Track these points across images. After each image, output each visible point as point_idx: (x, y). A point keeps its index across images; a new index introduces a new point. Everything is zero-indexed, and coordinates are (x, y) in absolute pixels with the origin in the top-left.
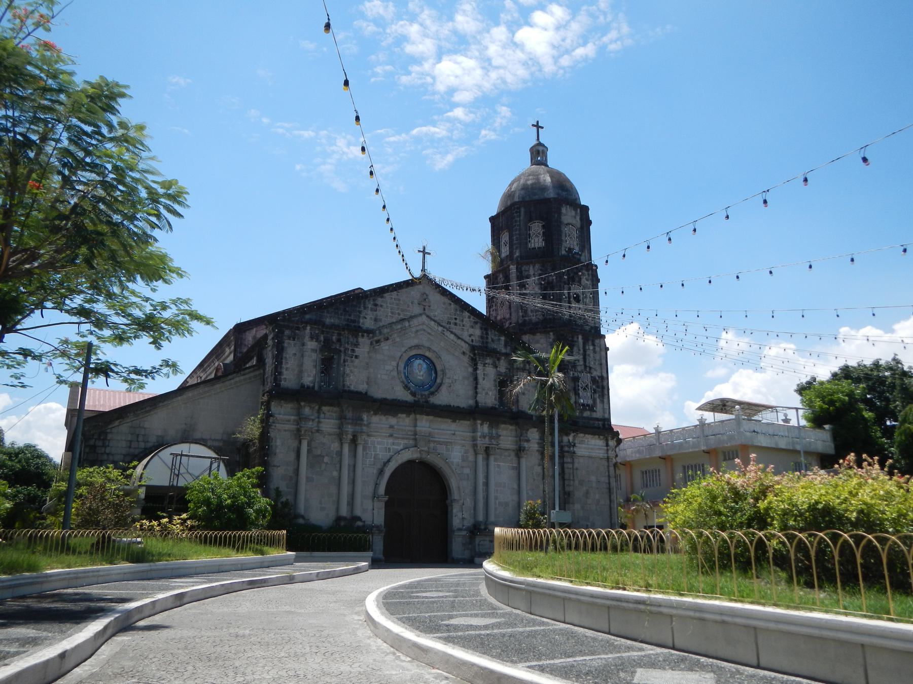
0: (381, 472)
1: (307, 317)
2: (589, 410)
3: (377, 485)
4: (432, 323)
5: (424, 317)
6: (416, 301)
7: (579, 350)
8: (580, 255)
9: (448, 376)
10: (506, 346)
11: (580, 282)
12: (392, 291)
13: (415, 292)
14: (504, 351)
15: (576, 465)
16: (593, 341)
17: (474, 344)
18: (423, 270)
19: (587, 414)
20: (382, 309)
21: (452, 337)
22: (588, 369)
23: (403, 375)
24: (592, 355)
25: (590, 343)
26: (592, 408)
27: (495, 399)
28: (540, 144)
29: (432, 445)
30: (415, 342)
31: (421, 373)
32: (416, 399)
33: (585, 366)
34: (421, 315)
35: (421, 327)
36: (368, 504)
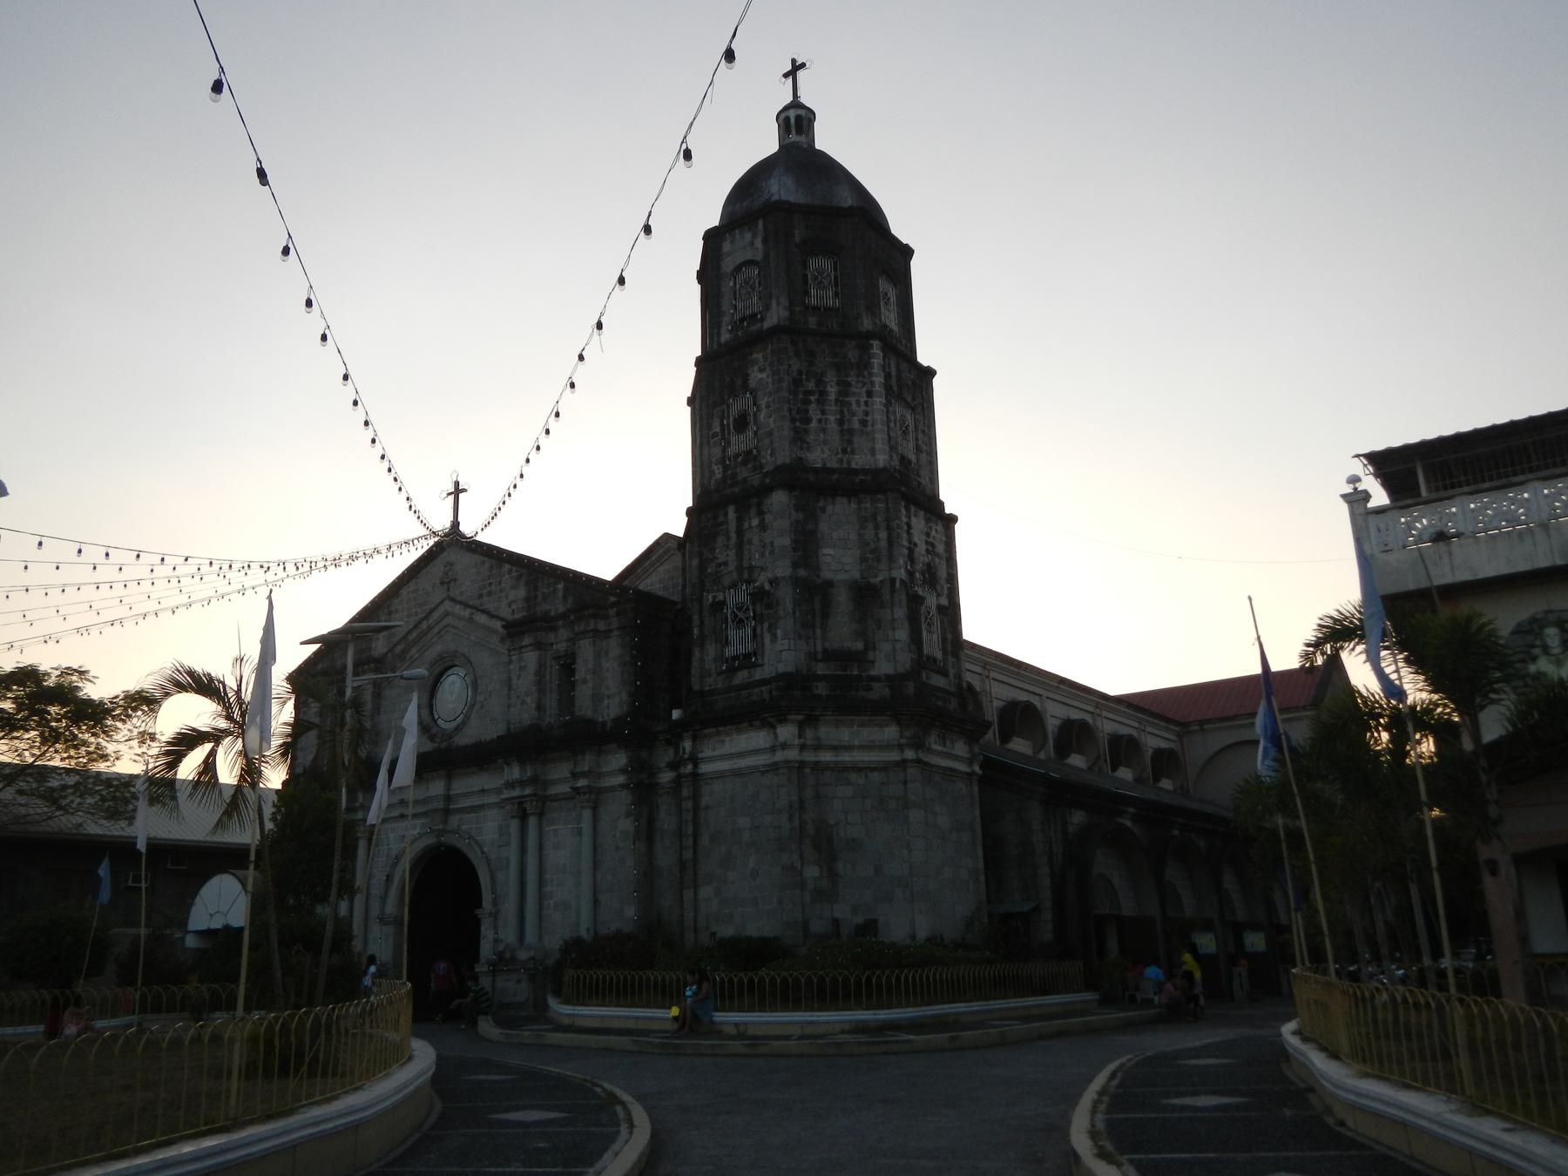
0: (389, 879)
1: (320, 666)
2: (740, 668)
3: (384, 898)
4: (458, 606)
5: (447, 605)
6: (438, 582)
7: (729, 539)
8: (762, 320)
9: (479, 691)
10: (565, 597)
11: (745, 387)
12: (408, 582)
13: (437, 568)
14: (561, 609)
15: (705, 800)
16: (759, 505)
17: (516, 616)
18: (455, 524)
19: (741, 677)
20: (397, 616)
21: (482, 619)
22: (746, 575)
23: (425, 712)
24: (756, 540)
25: (753, 511)
26: (747, 661)
27: (540, 707)
28: (796, 104)
29: (454, 821)
30: (439, 648)
31: (454, 696)
32: (436, 745)
33: (740, 569)
34: (442, 602)
35: (444, 623)
36: (376, 931)
